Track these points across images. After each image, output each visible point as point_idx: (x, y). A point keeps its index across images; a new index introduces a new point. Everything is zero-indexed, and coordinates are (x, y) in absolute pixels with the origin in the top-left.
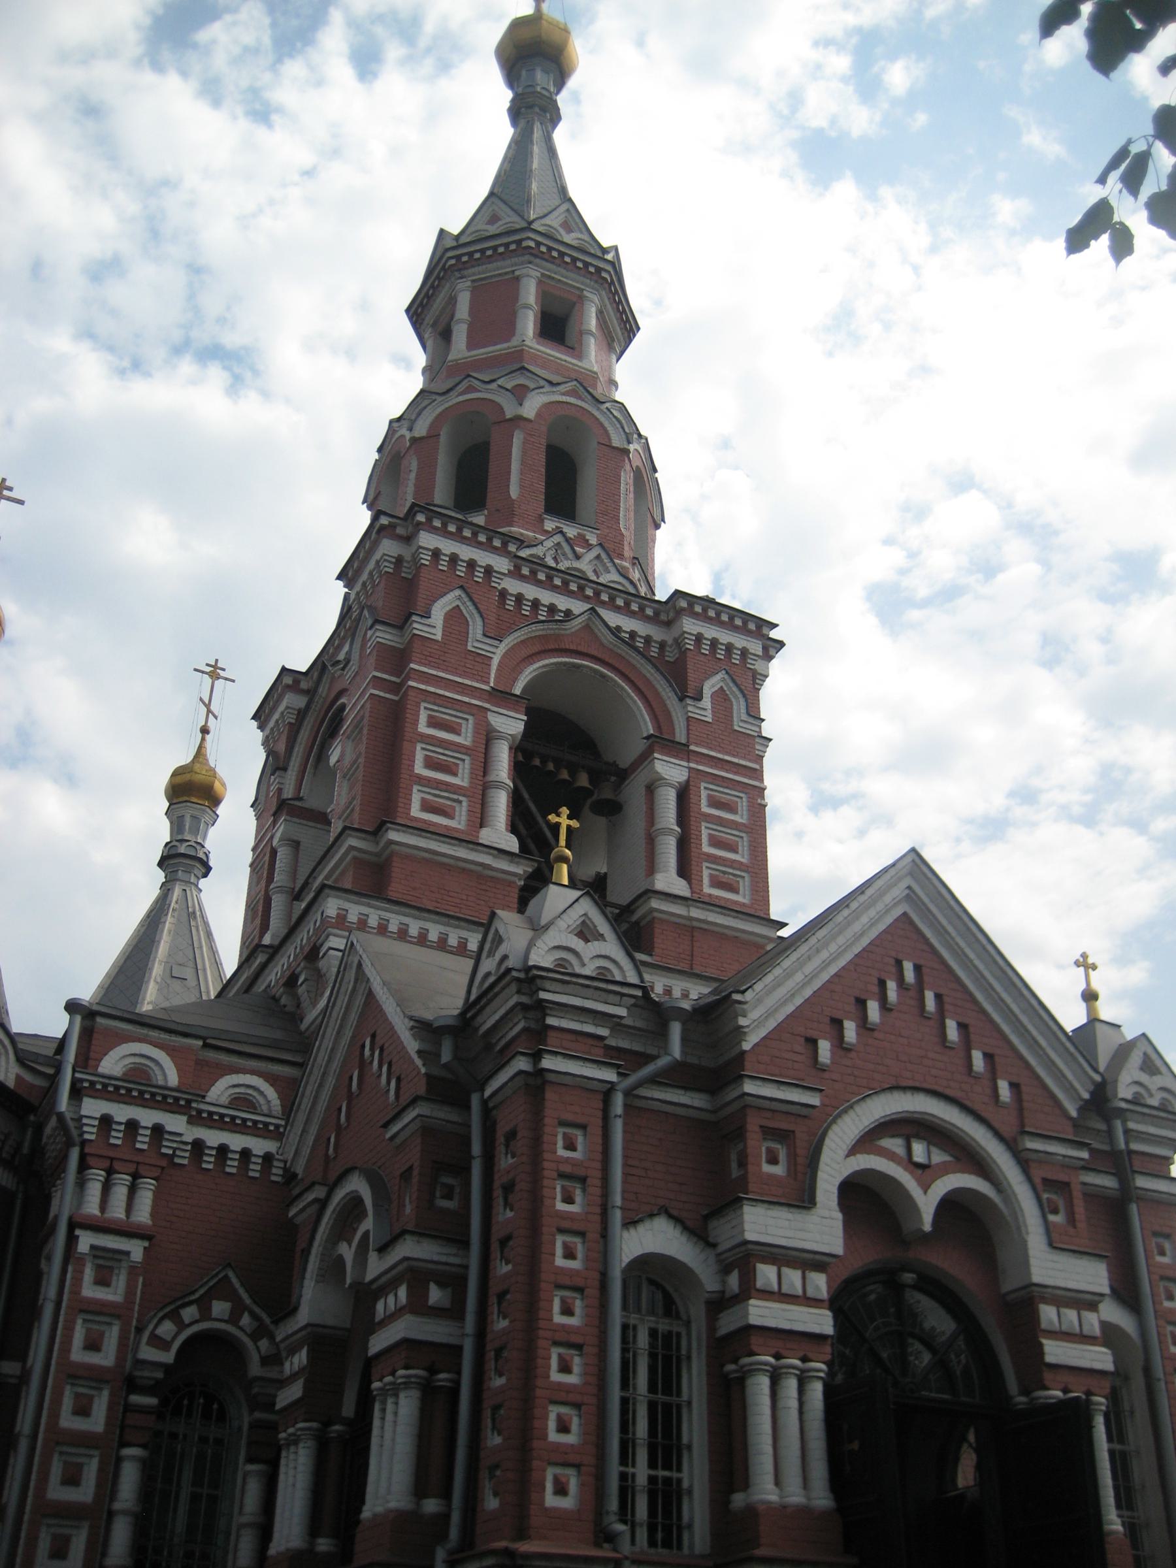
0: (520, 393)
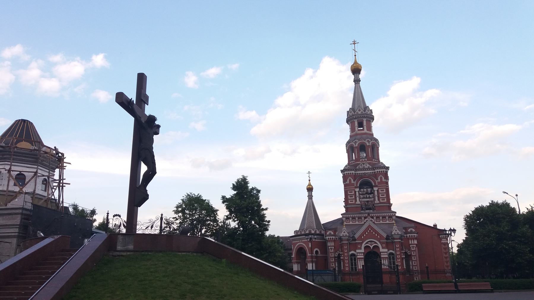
0: (356, 142)
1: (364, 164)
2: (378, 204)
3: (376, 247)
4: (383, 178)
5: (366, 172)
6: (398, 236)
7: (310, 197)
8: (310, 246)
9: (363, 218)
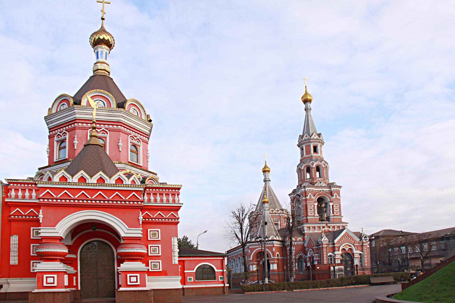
0: (313, 164)
2: (333, 216)
9: (321, 227)
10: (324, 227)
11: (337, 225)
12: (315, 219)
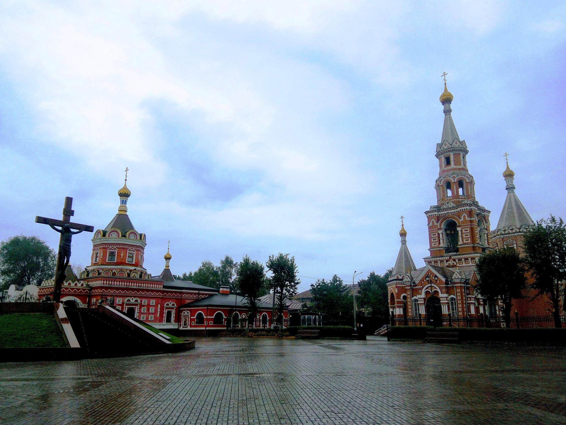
0: (440, 181)
1: (448, 203)
3: (436, 292)
4: (466, 216)
5: (450, 211)
6: (459, 281)
7: (404, 242)
8: (397, 291)
10: (447, 261)
11: (464, 256)
12: (440, 250)
